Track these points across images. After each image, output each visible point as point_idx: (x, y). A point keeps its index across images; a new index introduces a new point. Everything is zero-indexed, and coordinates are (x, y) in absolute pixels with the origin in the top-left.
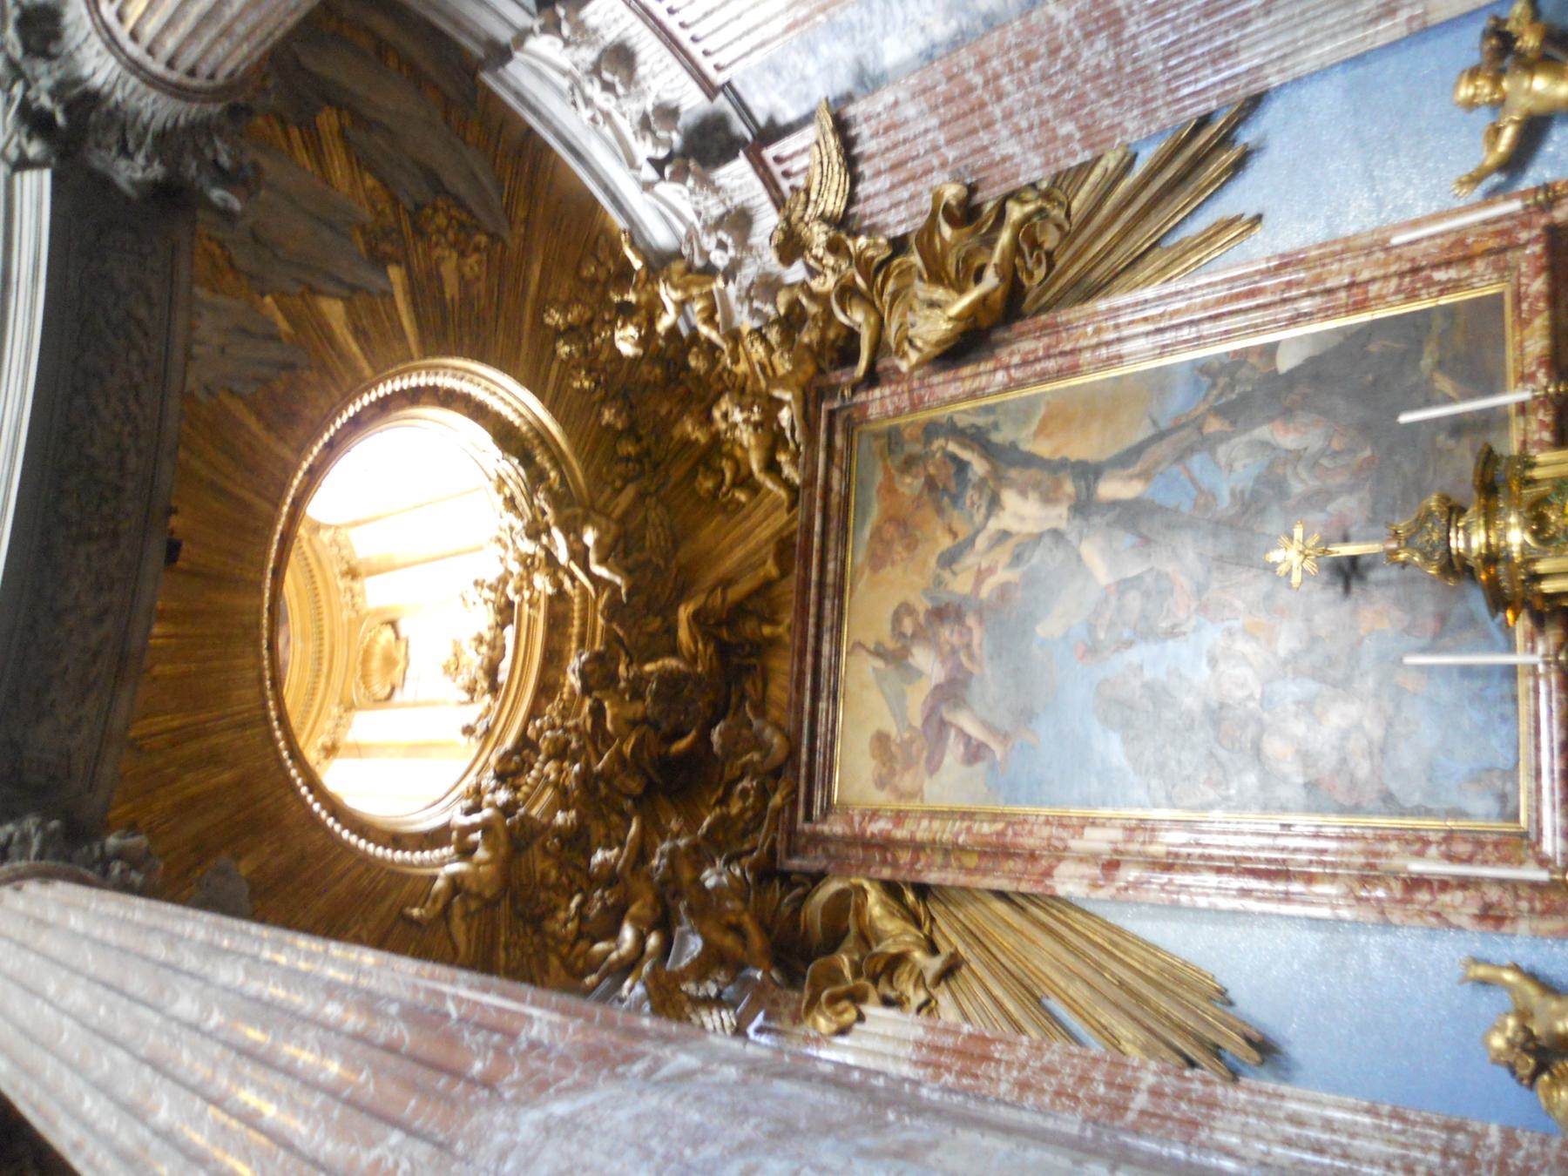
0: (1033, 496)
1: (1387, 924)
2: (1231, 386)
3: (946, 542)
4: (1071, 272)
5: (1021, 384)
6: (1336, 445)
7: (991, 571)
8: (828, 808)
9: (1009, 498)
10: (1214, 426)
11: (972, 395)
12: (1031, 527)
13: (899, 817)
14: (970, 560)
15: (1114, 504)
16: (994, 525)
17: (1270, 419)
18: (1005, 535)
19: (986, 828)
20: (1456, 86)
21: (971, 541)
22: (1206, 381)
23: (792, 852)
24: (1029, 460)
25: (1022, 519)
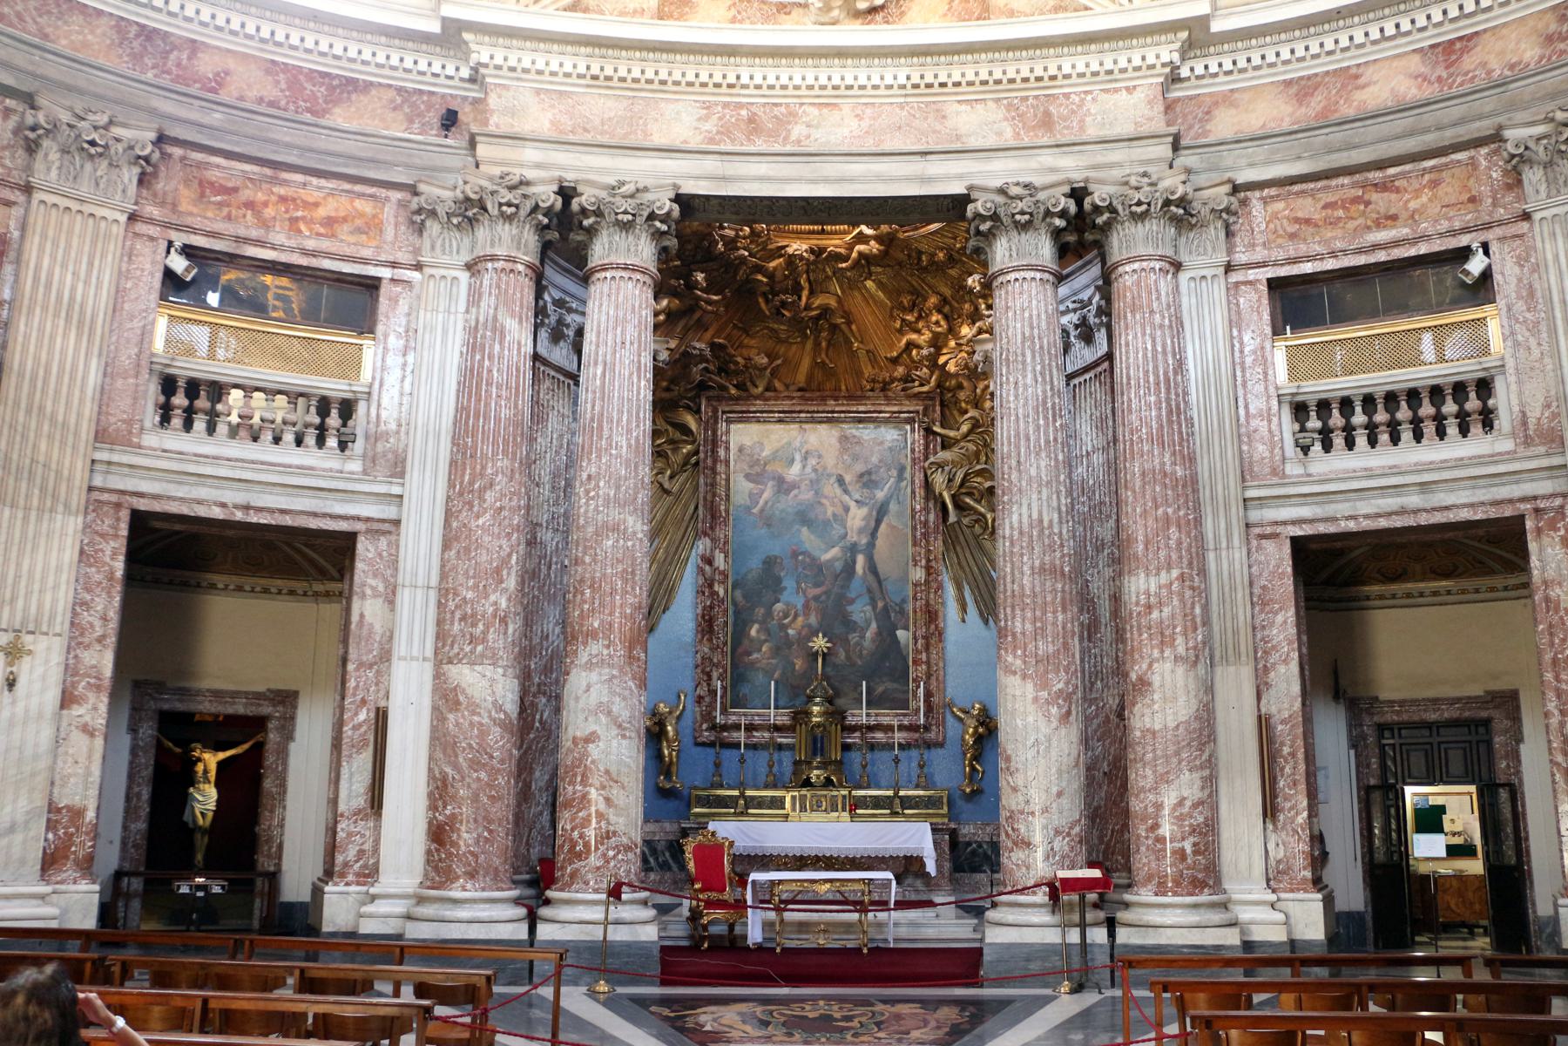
0: (863, 523)
1: (697, 667)
2: (896, 612)
3: (848, 478)
4: (961, 537)
5: (913, 517)
6: (865, 652)
7: (833, 505)
8: (729, 421)
9: (864, 511)
10: (880, 604)
11: (913, 492)
12: (849, 524)
13: (727, 462)
14: (838, 491)
15: (854, 562)
16: (852, 504)
17: (878, 627)
18: (847, 509)
19: (723, 508)
20: (980, 703)
21: (846, 491)
22: (898, 600)
23: (709, 399)
24: (878, 522)
25: (854, 518)
